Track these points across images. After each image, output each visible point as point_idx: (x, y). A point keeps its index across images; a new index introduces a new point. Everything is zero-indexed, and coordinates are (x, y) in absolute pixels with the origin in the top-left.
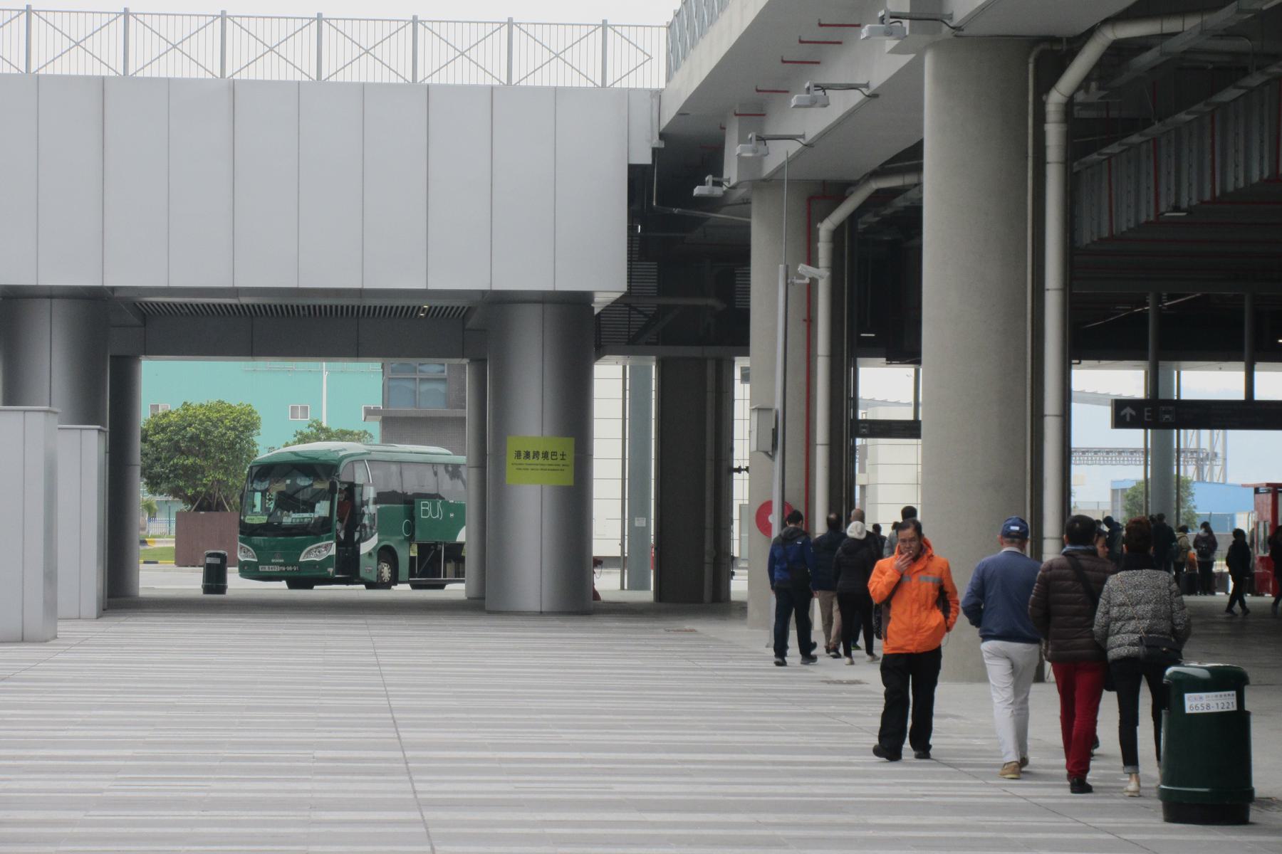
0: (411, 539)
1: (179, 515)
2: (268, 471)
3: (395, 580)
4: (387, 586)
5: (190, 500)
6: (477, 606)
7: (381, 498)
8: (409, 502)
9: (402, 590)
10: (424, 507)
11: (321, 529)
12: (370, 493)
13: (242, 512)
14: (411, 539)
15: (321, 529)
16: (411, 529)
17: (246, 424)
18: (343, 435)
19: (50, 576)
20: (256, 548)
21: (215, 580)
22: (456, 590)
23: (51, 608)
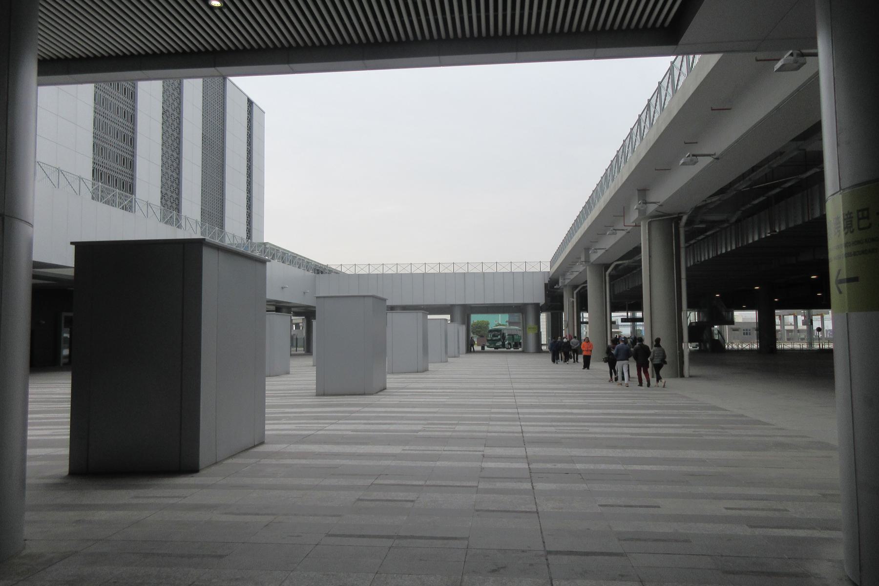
0: (513, 342)
1: (478, 338)
2: (491, 331)
3: (511, 348)
4: (510, 349)
5: (479, 336)
6: (523, 352)
7: (508, 335)
8: (513, 335)
9: (512, 349)
10: (515, 336)
11: (499, 340)
12: (507, 334)
13: (487, 337)
14: (513, 342)
15: (499, 340)
16: (513, 340)
17: (488, 324)
18: (503, 325)
19: (459, 348)
20: (490, 343)
21: (483, 348)
22: (520, 349)
23: (459, 353)
